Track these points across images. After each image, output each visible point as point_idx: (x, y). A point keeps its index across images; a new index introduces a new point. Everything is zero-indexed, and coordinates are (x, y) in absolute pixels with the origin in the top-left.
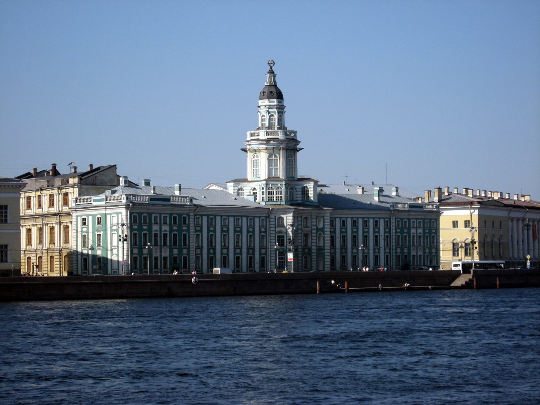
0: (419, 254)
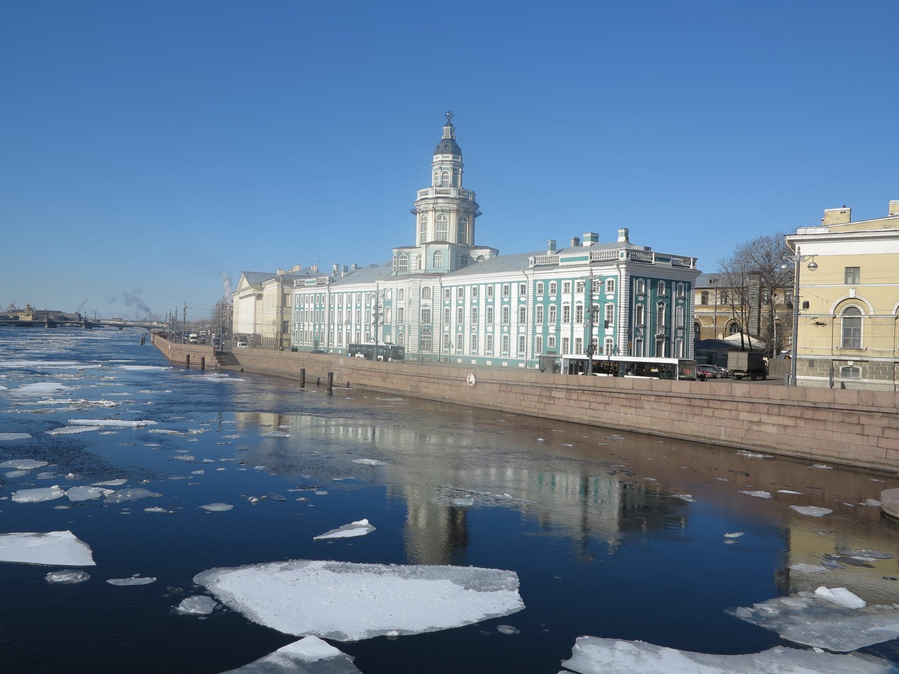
0: (576, 336)
